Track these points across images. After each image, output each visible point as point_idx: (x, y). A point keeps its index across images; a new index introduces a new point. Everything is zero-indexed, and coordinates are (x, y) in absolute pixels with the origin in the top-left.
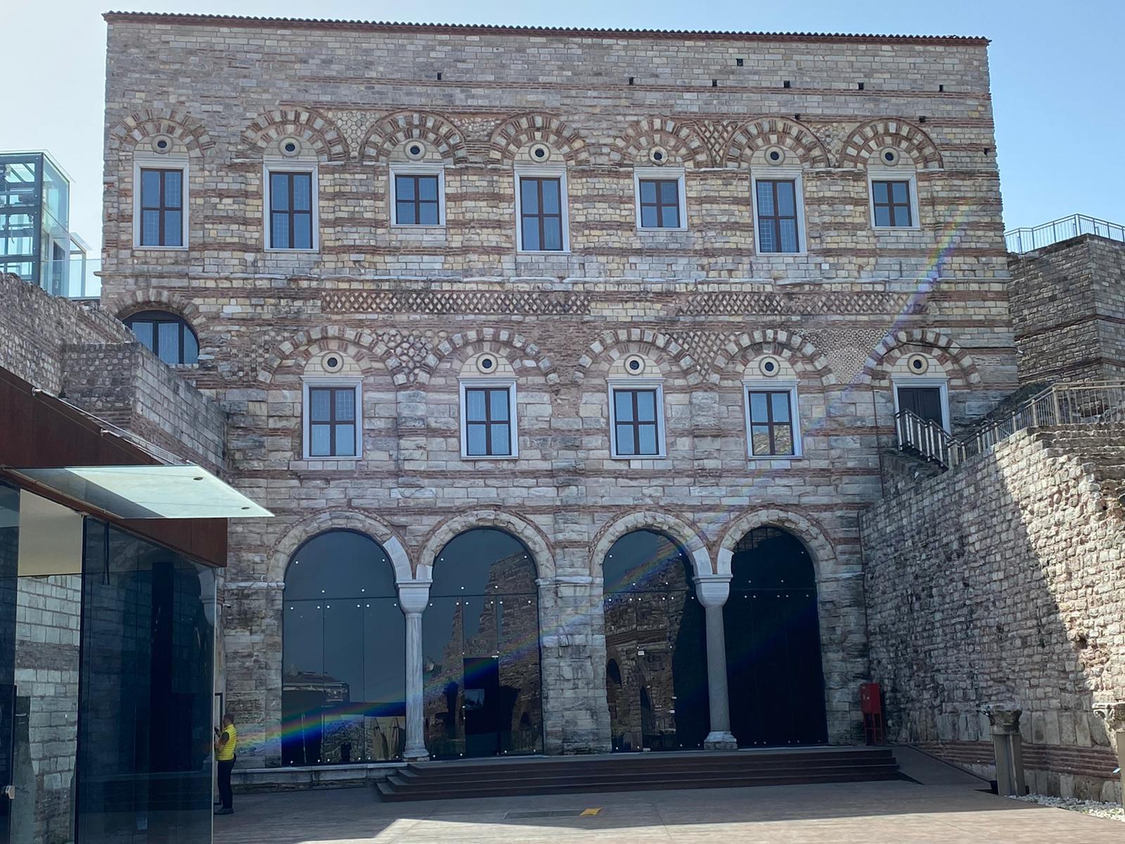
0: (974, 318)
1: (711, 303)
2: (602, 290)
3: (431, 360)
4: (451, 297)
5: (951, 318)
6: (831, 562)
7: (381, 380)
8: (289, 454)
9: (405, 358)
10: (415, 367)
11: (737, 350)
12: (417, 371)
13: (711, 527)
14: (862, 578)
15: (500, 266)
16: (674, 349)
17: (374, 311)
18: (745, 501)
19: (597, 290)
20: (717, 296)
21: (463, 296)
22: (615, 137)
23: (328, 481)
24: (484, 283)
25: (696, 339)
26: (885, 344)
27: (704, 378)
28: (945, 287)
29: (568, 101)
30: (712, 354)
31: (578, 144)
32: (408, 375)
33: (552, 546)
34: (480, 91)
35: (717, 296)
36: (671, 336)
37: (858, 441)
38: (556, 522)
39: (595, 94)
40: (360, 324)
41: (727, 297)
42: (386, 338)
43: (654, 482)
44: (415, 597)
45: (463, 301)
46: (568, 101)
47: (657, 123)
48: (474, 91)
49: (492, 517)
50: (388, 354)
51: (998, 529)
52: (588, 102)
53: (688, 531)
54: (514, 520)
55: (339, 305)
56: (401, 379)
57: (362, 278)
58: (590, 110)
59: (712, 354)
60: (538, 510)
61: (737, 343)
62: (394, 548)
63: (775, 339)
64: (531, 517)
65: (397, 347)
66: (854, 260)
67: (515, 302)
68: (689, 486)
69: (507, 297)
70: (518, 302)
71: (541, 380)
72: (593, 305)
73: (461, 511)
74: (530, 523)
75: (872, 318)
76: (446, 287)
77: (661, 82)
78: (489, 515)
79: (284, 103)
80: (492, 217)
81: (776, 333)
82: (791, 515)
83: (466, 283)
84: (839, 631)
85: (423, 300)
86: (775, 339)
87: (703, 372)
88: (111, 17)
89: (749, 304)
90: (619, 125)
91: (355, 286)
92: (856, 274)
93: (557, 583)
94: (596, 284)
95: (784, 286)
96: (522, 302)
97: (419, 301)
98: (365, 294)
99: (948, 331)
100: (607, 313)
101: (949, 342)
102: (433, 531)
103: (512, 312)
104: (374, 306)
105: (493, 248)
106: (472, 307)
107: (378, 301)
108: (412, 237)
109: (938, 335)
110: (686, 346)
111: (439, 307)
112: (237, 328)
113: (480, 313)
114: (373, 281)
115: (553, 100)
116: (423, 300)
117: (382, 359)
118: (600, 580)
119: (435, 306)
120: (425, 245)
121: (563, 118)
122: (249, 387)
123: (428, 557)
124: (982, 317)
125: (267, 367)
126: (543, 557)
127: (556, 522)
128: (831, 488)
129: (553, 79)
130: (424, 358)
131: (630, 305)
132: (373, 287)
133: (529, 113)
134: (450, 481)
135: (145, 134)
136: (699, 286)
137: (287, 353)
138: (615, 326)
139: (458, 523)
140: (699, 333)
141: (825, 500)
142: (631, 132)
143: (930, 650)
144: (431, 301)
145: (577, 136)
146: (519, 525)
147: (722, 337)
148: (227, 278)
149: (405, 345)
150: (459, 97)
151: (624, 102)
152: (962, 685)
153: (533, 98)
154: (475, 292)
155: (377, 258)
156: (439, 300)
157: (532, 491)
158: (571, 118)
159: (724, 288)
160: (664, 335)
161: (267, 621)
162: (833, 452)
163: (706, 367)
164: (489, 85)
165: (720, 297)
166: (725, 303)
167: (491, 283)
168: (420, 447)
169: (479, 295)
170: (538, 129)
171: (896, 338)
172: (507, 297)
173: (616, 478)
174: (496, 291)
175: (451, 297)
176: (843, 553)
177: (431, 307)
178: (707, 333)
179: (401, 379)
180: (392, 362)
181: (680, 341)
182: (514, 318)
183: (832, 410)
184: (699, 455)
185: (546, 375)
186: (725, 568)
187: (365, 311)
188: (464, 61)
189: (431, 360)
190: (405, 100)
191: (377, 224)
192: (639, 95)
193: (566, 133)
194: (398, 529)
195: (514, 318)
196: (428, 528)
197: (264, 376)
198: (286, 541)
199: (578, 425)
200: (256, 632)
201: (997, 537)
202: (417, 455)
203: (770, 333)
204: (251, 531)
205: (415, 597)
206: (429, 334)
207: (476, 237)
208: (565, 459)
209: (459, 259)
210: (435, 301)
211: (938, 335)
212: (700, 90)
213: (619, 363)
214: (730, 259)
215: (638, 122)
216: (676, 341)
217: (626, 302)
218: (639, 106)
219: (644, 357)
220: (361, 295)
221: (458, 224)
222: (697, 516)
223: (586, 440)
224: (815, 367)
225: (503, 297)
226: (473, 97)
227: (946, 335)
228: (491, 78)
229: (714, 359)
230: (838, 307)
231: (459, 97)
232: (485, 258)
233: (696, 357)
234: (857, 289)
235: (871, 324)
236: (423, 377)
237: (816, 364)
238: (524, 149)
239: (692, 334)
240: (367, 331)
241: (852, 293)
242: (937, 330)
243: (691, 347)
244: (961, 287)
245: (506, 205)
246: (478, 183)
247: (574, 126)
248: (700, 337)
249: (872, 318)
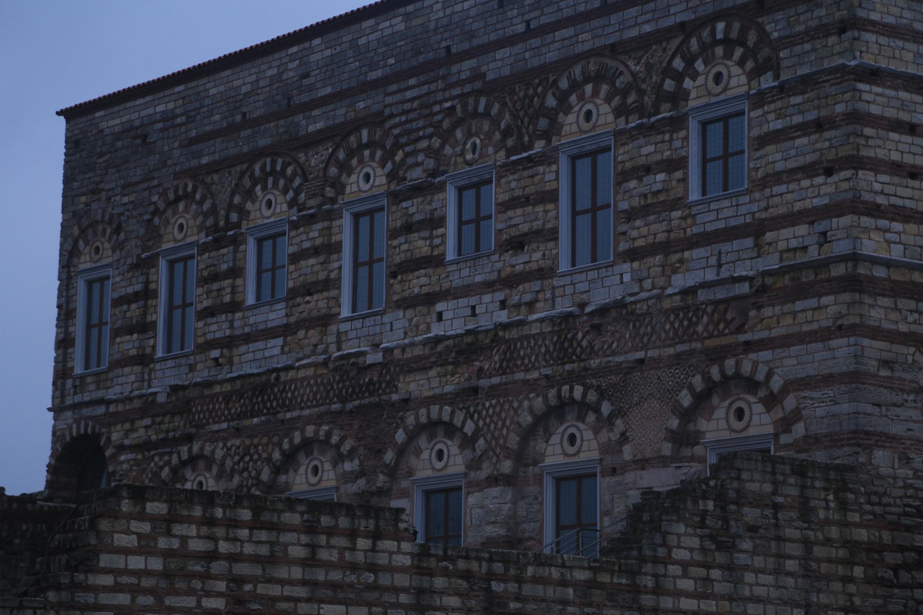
11: (529, 419)
16: (469, 428)
29: (389, 100)
46: (389, 100)
52: (409, 94)
65: (239, 462)
77: (476, 42)
79: (177, 176)
88: (69, 114)
94: (403, 350)
99: (766, 355)
100: (412, 387)
105: (319, 318)
108: (260, 318)
120: (270, 325)
133: (354, 126)
135: (86, 243)
147: (516, 404)
148: (130, 399)
160: (461, 409)
178: (501, 400)
181: (476, 416)
190: (262, 143)
191: (235, 306)
206: (265, 440)
211: (755, 364)
213: (425, 455)
216: (472, 418)
219: (449, 442)
221: (293, 294)
238: (354, 178)
239: (487, 404)
249: (680, 348)
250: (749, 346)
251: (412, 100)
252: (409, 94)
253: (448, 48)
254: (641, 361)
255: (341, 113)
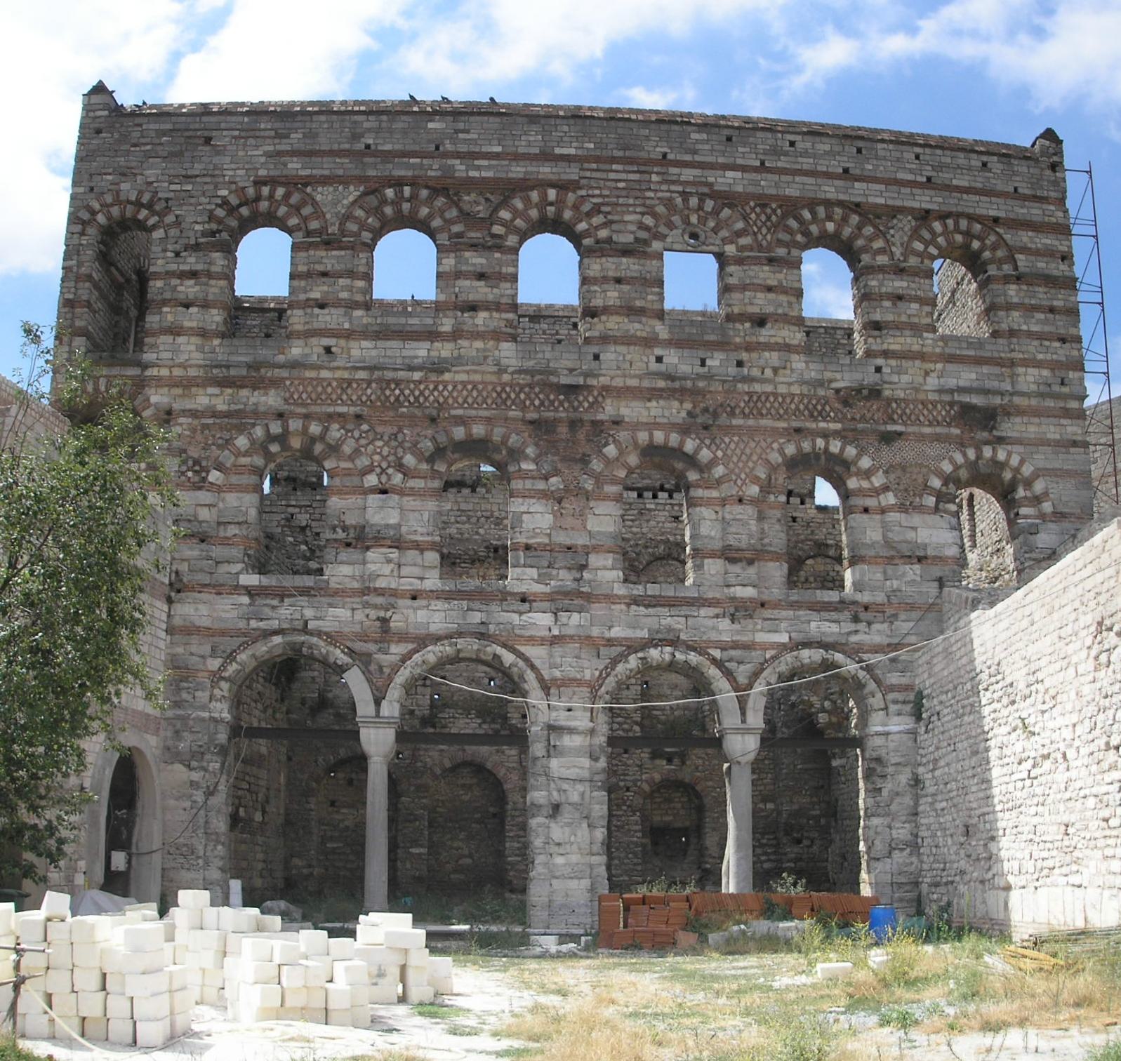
0: (1049, 436)
1: (751, 404)
2: (621, 385)
3: (409, 460)
4: (436, 388)
5: (1024, 435)
6: (881, 713)
7: (348, 482)
8: (240, 566)
9: (377, 457)
10: (389, 466)
11: (780, 460)
12: (390, 471)
13: (742, 667)
14: (913, 733)
15: (497, 353)
17: (344, 403)
18: (783, 638)
19: (614, 384)
20: (759, 397)
21: (450, 388)
22: (643, 214)
23: (282, 598)
24: (475, 372)
25: (733, 446)
26: (952, 461)
27: (740, 488)
28: (1017, 400)
29: (588, 174)
30: (750, 464)
31: (597, 220)
32: (379, 475)
33: (546, 687)
34: (485, 163)
35: (759, 397)
36: (702, 442)
37: (918, 572)
38: (551, 656)
39: (620, 167)
40: (331, 417)
41: (772, 399)
42: (356, 434)
43: (675, 611)
44: (378, 742)
45: (451, 393)
46: (588, 174)
47: (694, 202)
48: (476, 162)
49: (475, 647)
50: (357, 452)
51: (1074, 659)
52: (612, 176)
53: (713, 672)
54: (500, 650)
55: (304, 396)
56: (372, 480)
57: (335, 364)
58: (612, 184)
59: (750, 464)
60: (531, 640)
61: (781, 451)
62: (355, 681)
63: (826, 449)
64: (522, 649)
66: (917, 363)
67: (513, 396)
68: (717, 616)
69: (503, 390)
70: (518, 395)
71: (541, 485)
72: (609, 401)
73: (437, 639)
74: (520, 655)
75: (938, 430)
76: (433, 377)
78: (469, 646)
80: (490, 297)
81: (827, 443)
82: (839, 657)
83: (456, 372)
84: (885, 793)
85: (402, 392)
86: (826, 449)
87: (739, 482)
89: (797, 408)
90: (648, 202)
91: (325, 374)
92: (921, 380)
93: (552, 728)
94: (612, 378)
95: (837, 391)
96: (522, 396)
97: (397, 392)
98: (334, 384)
99: (1020, 449)
101: (1022, 462)
102: (403, 660)
103: (509, 408)
104: (344, 397)
106: (460, 400)
107: (349, 391)
109: (1009, 454)
110: (720, 454)
111: (421, 400)
112: (190, 420)
113: (471, 407)
114: (346, 369)
115: (572, 173)
116: (402, 392)
117: (351, 458)
118: (603, 728)
119: (417, 399)
120: (409, 329)
121: (583, 193)
122: (200, 488)
123: (395, 693)
124: (1058, 437)
125: (220, 467)
126: (535, 698)
127: (551, 656)
128: (886, 625)
129: (572, 151)
130: (402, 458)
131: (654, 403)
132: (346, 375)
134: (424, 602)
136: (739, 385)
137: (243, 449)
138: (637, 426)
139: (431, 654)
140: (736, 439)
141: (877, 639)
142: (661, 209)
143: (984, 814)
144: (412, 392)
145: (596, 210)
146: (508, 658)
148: (184, 366)
149: (380, 443)
150: (459, 167)
151: (654, 178)
152: (1019, 855)
153: (546, 171)
154: (464, 384)
155: (353, 344)
156: (422, 393)
157: (524, 617)
158: (590, 192)
159: (769, 388)
161: (208, 757)
162: (888, 583)
163: (743, 476)
164: (497, 156)
165: (763, 398)
166: (768, 405)
167: (483, 372)
168: (389, 561)
169: (470, 387)
170: (551, 204)
171: (965, 455)
172: (503, 390)
173: (628, 605)
174: (491, 383)
175: (436, 388)
176: (895, 702)
177: (412, 399)
179: (372, 480)
180: (363, 462)
182: (511, 414)
183: (890, 535)
184: (732, 580)
185: (547, 479)
186: (756, 719)
187: (334, 403)
188: (467, 132)
189: (409, 460)
192: (673, 170)
193: (586, 207)
194: (364, 660)
195: (511, 414)
196: (398, 658)
197: (214, 476)
198: (232, 668)
199: (581, 540)
200: (194, 769)
201: (1071, 671)
202: (387, 569)
203: (820, 443)
204: (192, 654)
205: (378, 742)
207: (471, 322)
208: (565, 578)
209: (450, 346)
210: (417, 393)
211: (1009, 454)
212: (744, 169)
214: (775, 355)
215: (670, 200)
216: (709, 447)
217: (649, 400)
218: (673, 182)
220: (330, 384)
222: (727, 655)
223: (594, 560)
224: (871, 483)
225: (499, 389)
226: (479, 168)
227: (1019, 454)
228: (499, 149)
229: (753, 469)
230: (901, 416)
231: (459, 167)
232: (479, 344)
233: (731, 466)
234: (921, 396)
235: (937, 438)
236: (398, 478)
237: (873, 479)
240: (336, 426)
241: (915, 401)
242: (1009, 447)
243: (725, 454)
244: (1034, 402)
245: (508, 285)
246: (476, 260)
247: (595, 200)
248: (737, 444)
249: (938, 430)
250: (1001, 440)
251: (620, 181)
252: (612, 176)
253: (665, 155)
254: (900, 434)
255: (518, 171)
